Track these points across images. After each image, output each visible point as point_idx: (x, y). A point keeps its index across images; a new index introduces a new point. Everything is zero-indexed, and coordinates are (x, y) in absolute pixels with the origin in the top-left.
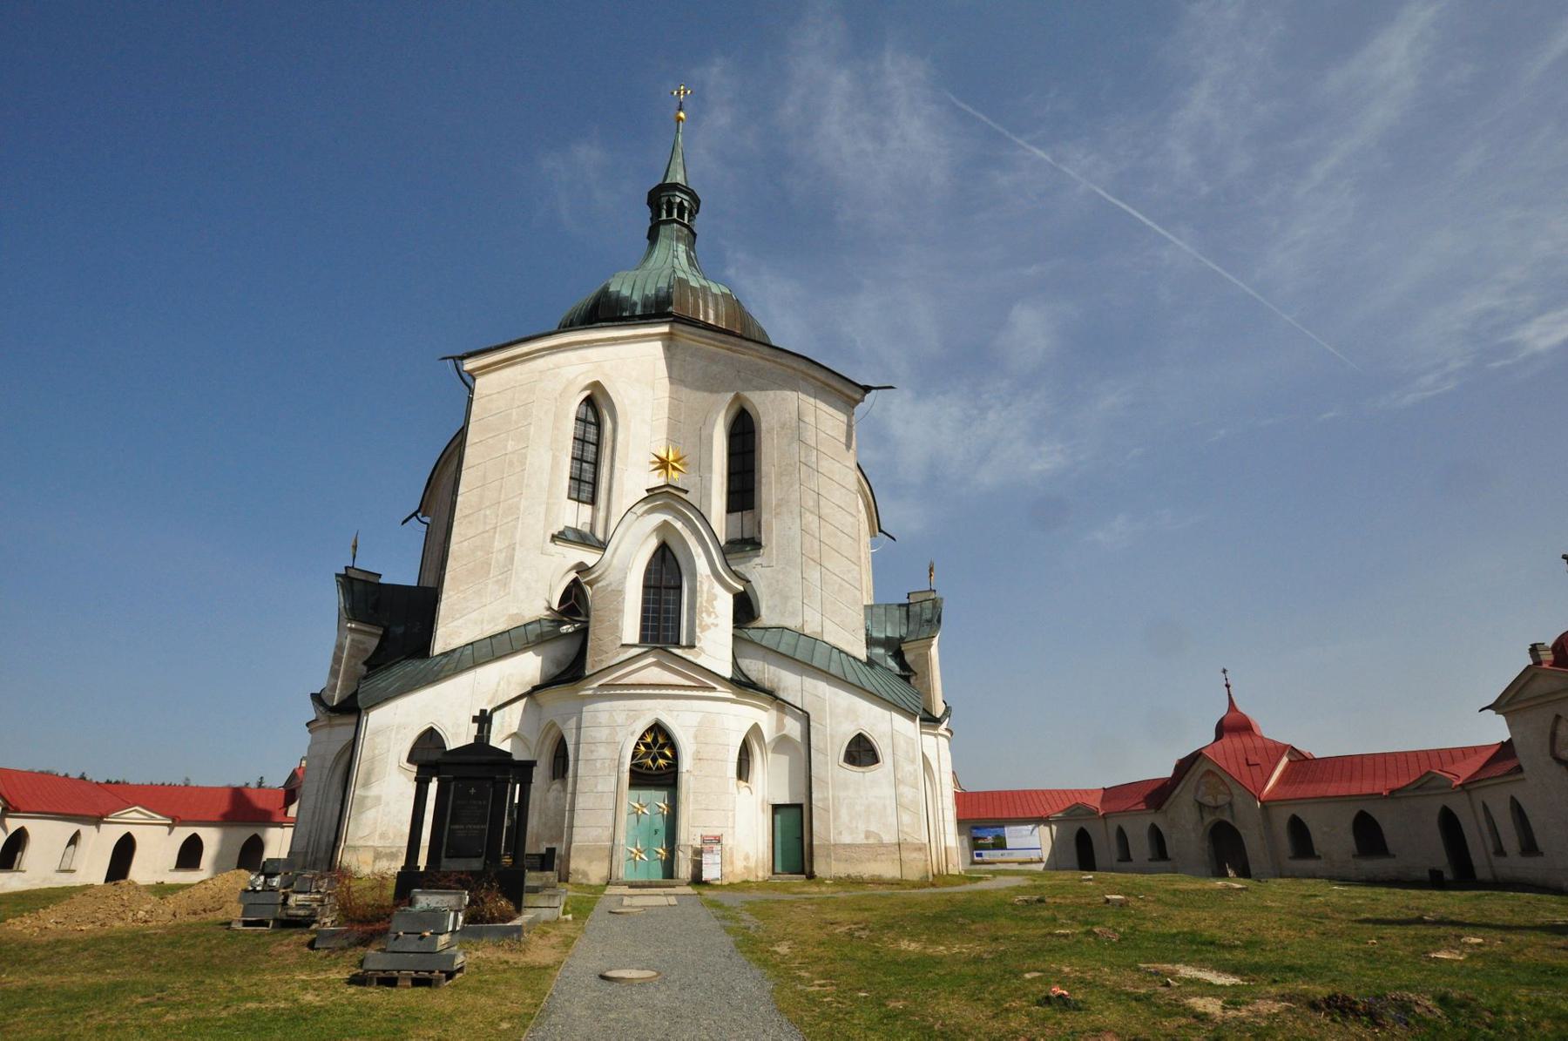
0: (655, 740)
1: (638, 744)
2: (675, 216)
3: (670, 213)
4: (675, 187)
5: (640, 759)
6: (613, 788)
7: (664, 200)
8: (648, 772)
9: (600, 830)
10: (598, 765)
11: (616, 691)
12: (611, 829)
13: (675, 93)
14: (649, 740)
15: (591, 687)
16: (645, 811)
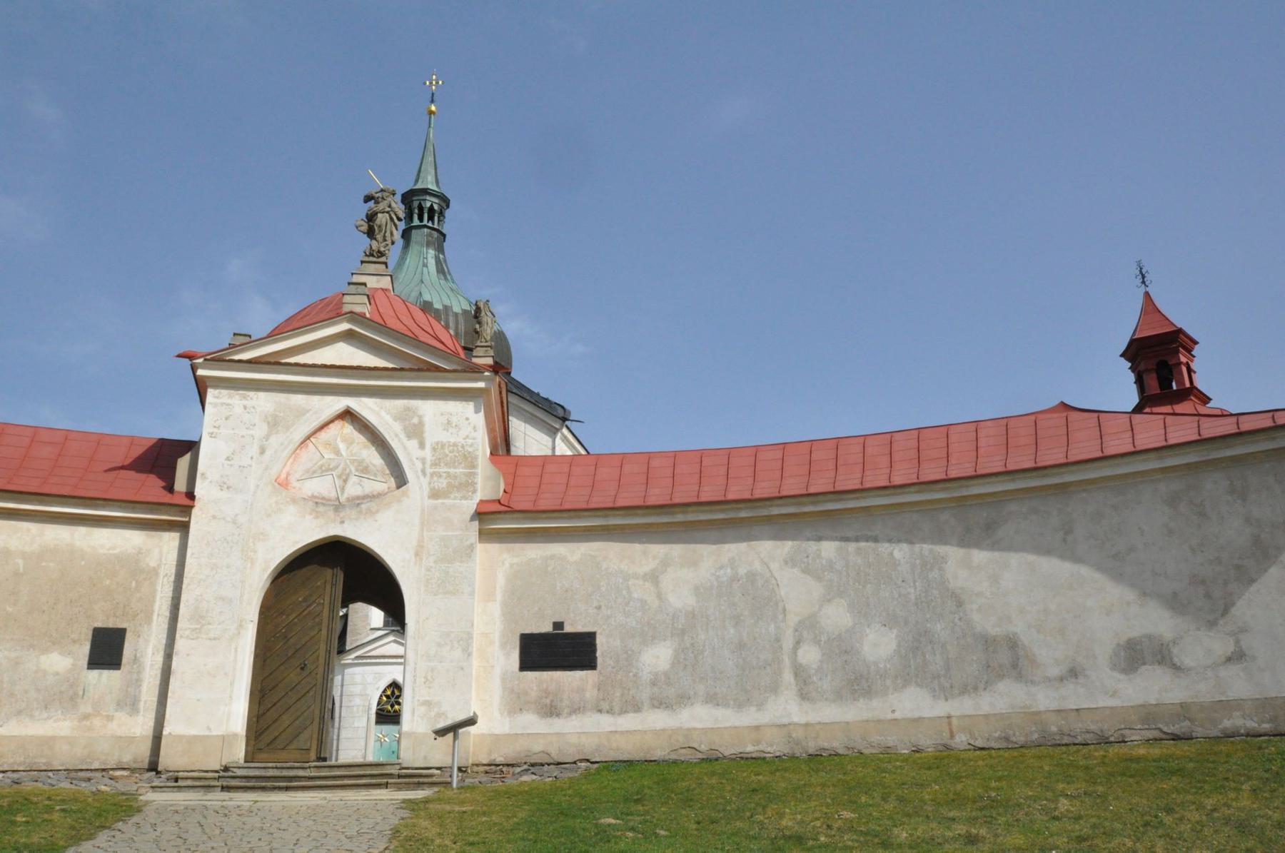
0: (393, 693)
1: (381, 696)
2: (425, 222)
3: (421, 219)
4: (425, 191)
5: (383, 705)
6: (365, 725)
7: (416, 204)
8: (389, 714)
9: (356, 752)
10: (355, 709)
11: (365, 660)
12: (364, 751)
13: (428, 83)
14: (389, 693)
15: (350, 657)
16: (386, 739)
